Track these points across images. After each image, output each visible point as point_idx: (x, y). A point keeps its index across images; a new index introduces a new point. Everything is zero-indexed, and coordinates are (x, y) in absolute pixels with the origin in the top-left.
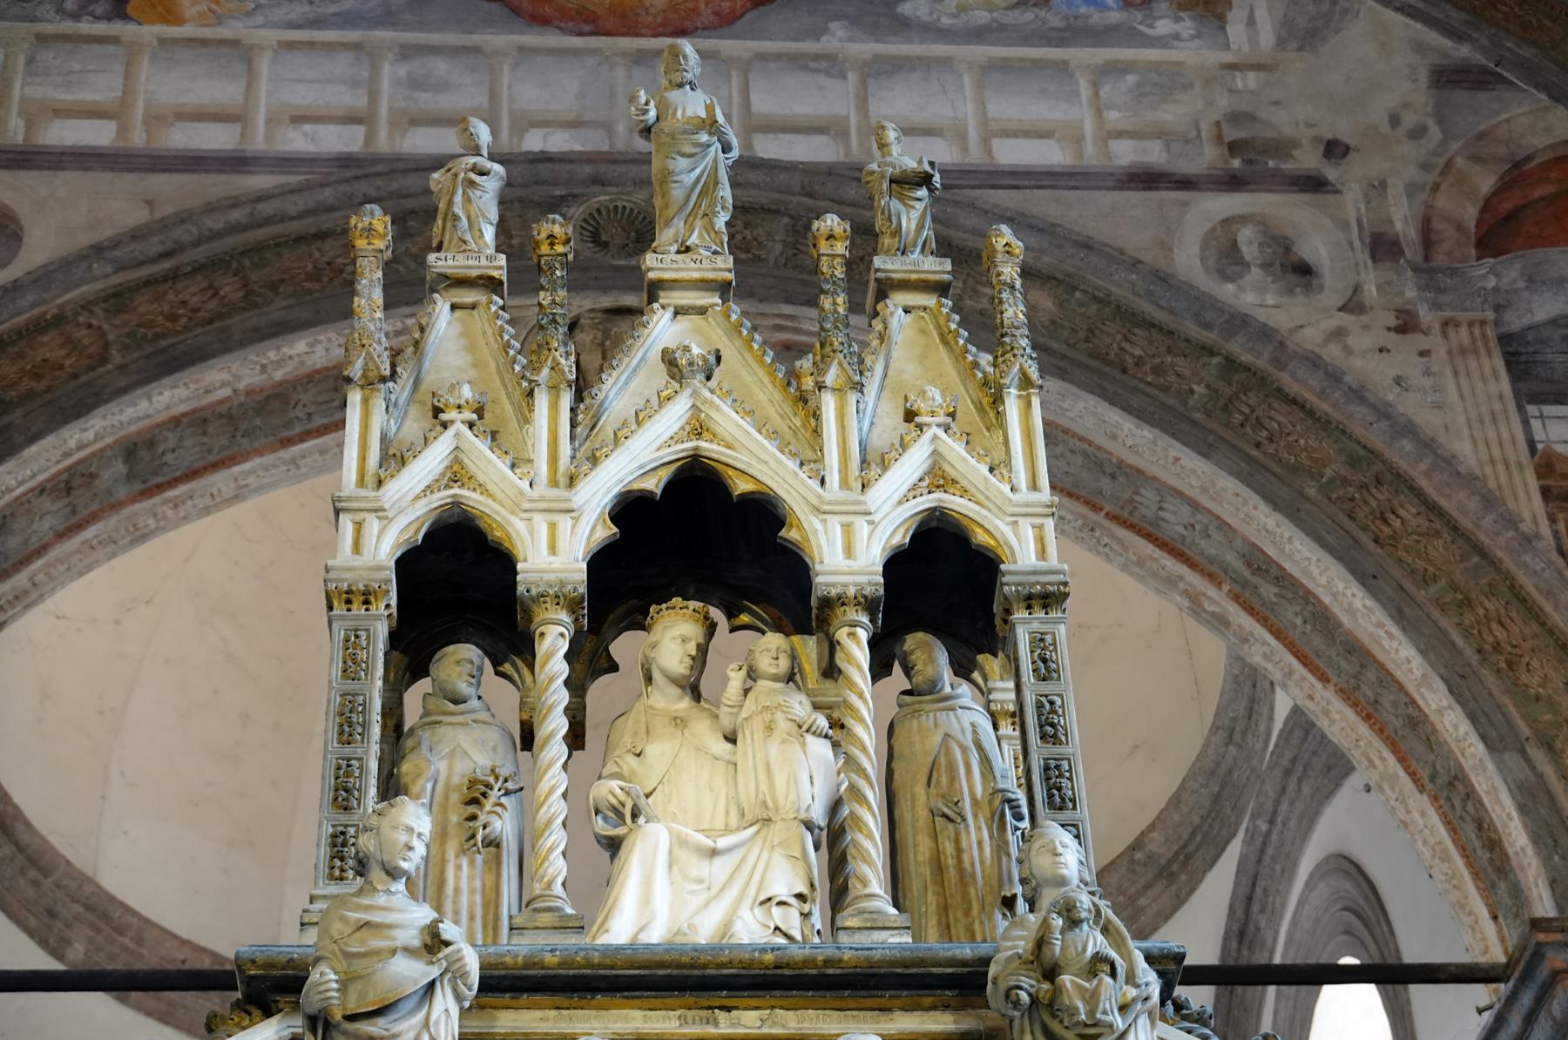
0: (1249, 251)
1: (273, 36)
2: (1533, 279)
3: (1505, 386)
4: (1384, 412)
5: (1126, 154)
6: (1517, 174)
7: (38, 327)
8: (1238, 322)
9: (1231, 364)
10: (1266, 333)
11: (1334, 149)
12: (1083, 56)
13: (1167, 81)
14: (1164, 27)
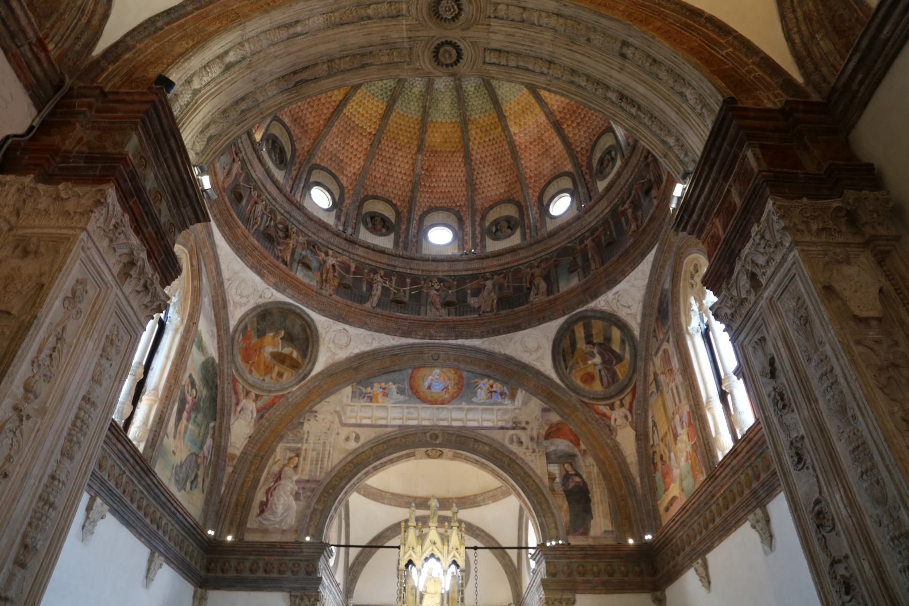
0: (515, 440)
1: (391, 405)
2: (551, 444)
3: (545, 461)
4: (529, 466)
5: (500, 424)
6: (551, 427)
7: (362, 453)
8: (512, 452)
9: (511, 458)
10: (515, 454)
11: (527, 423)
12: (496, 407)
13: (506, 412)
14: (507, 402)
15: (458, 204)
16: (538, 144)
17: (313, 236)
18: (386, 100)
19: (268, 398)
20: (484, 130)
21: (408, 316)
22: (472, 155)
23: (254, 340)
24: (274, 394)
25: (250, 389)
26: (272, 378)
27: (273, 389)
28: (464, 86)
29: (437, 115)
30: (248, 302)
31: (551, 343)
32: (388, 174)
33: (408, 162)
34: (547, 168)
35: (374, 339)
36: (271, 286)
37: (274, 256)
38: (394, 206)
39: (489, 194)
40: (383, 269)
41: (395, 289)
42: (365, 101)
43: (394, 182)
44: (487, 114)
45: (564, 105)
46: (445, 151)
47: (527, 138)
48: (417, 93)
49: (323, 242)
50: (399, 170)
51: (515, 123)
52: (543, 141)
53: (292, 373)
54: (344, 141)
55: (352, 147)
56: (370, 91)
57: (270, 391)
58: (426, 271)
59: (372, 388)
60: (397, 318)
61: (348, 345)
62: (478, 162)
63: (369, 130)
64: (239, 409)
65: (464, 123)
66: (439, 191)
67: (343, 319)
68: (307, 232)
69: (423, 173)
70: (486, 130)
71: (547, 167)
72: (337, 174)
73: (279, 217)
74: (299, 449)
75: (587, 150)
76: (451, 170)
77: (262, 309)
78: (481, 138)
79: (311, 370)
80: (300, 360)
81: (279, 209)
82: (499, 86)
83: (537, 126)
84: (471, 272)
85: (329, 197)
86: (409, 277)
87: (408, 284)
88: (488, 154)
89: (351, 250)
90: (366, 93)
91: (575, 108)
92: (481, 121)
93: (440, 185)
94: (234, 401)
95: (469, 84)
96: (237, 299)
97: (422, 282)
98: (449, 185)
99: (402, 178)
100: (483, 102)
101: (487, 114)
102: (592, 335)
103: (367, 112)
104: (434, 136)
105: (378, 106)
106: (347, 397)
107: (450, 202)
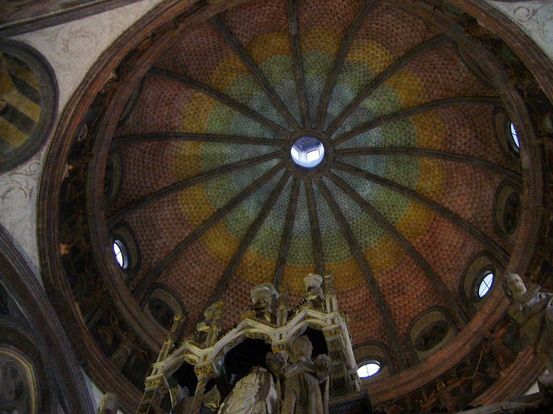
31: (53, 65)
44: (231, 83)
45: (165, 150)
48: (311, 70)
52: (166, 105)
54: (388, 28)
56: (364, 67)
70: (225, 71)
83: (178, 110)
90: (368, 66)
95: (260, 96)
100: (240, 90)
101: (231, 83)
102: (11, 121)
104: (280, 43)
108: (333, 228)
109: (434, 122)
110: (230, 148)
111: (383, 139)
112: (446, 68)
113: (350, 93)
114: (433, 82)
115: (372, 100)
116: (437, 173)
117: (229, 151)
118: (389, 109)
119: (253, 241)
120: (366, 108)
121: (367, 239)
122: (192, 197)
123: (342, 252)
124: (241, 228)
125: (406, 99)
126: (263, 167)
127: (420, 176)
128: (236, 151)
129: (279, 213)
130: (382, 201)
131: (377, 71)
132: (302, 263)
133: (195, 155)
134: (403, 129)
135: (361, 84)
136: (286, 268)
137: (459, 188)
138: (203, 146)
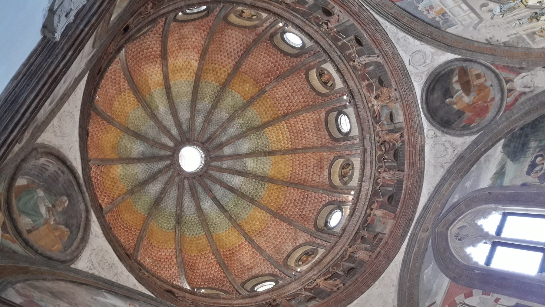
15: (266, 44)
16: (184, 45)
17: (370, 120)
18: (263, 132)
19: (502, 73)
20: (215, 72)
21: (362, 31)
22: (233, 65)
23: (468, 114)
24: (497, 71)
25: (506, 91)
26: (485, 81)
27: (493, 75)
28: (210, 105)
29: (238, 99)
30: (446, 141)
32: (294, 92)
33: (277, 89)
34: (187, 29)
35: (398, 39)
36: (424, 135)
37: (404, 144)
38: (307, 75)
39: (240, 35)
40: (348, 63)
41: (353, 48)
42: (274, 139)
43: (295, 85)
46: (249, 76)
47: (189, 53)
49: (368, 111)
50: (286, 89)
51: (191, 66)
52: (179, 46)
53: (470, 69)
54: (304, 131)
55: (302, 124)
57: (497, 76)
58: (323, 37)
59: (435, 18)
60: (371, 37)
61: (418, 51)
62: (233, 58)
63: (285, 125)
64: (527, 90)
65: (224, 86)
66: (271, 58)
67: (404, 71)
68: (371, 127)
69: (272, 78)
70: (213, 71)
71: (188, 29)
72: (323, 120)
73: (379, 153)
74: (528, 35)
75: (152, 32)
76: (253, 64)
77: (443, 129)
78: (220, 69)
79: (457, 60)
80: (457, 71)
81: (374, 155)
82: (187, 93)
83: (177, 57)
84: (294, 13)
85: (339, 118)
86: (338, 44)
87: (342, 42)
88: (223, 57)
89: (357, 91)
91: (143, 59)
92: (213, 78)
93: (267, 61)
94: (523, 98)
95: (206, 104)
96: (450, 150)
97: (332, 34)
98: (262, 57)
99: (288, 84)
101: (206, 80)
103: (278, 133)
104: (249, 90)
105: (270, 131)
106: (457, 28)
107: (270, 48)
108: (169, 208)
109: (278, 196)
110: (164, 109)
111: (240, 186)
112: (313, 172)
113: (246, 150)
114: (298, 174)
115: (253, 162)
116: (258, 223)
117: (161, 110)
118: (259, 172)
119: (124, 165)
120: (245, 164)
121: (186, 230)
122: (125, 104)
123: (165, 225)
124: (124, 153)
125: (273, 174)
126: (163, 139)
127: (245, 219)
128: (163, 114)
129: (148, 171)
130: (210, 217)
131: (274, 149)
132: (138, 208)
133: (150, 88)
134: (256, 189)
135: (257, 149)
136: (128, 200)
137: (268, 237)
138: (159, 90)
